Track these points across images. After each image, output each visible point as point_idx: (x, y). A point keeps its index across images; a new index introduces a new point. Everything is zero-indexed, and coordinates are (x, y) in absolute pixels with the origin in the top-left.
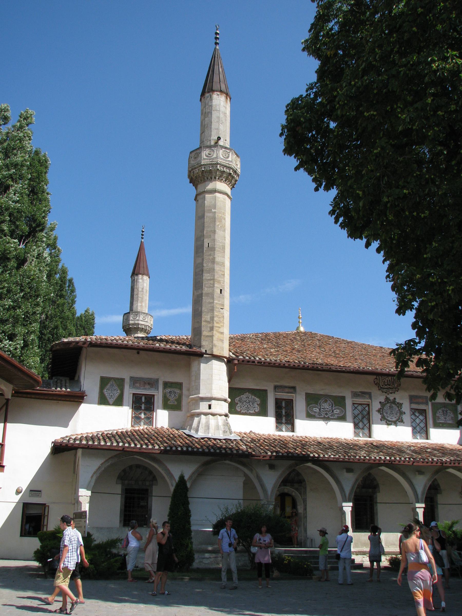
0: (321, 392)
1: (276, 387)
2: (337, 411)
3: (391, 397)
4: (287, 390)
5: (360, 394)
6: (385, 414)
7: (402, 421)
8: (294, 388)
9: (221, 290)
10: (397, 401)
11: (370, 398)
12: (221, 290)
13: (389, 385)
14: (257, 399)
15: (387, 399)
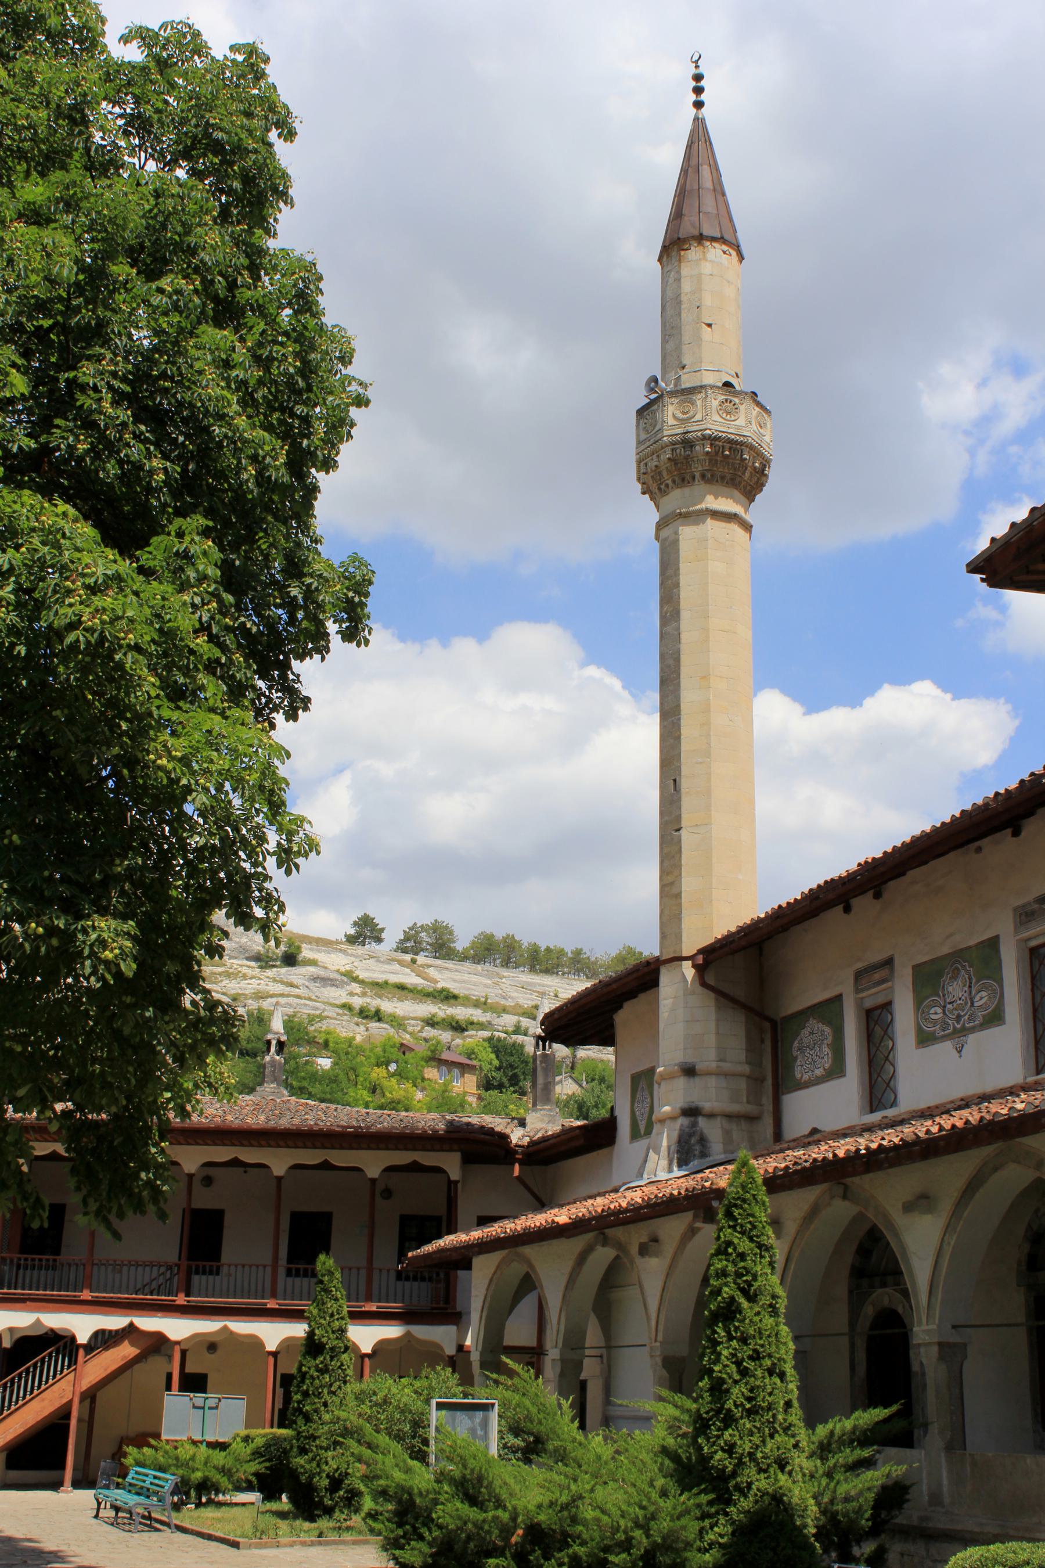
0: (946, 950)
2: (982, 998)
4: (877, 976)
5: (1036, 906)
8: (889, 962)
9: (675, 780)
12: (675, 780)
14: (827, 1030)
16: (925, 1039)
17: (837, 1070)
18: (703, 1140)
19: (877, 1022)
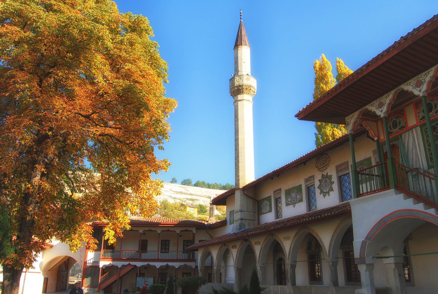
0: (291, 187)
1: (274, 192)
2: (298, 197)
3: (325, 173)
6: (322, 188)
7: (332, 190)
8: (280, 189)
10: (329, 174)
11: (314, 180)
13: (324, 164)
15: (323, 175)
16: (287, 205)
17: (270, 211)
18: (244, 225)
19: (277, 201)
